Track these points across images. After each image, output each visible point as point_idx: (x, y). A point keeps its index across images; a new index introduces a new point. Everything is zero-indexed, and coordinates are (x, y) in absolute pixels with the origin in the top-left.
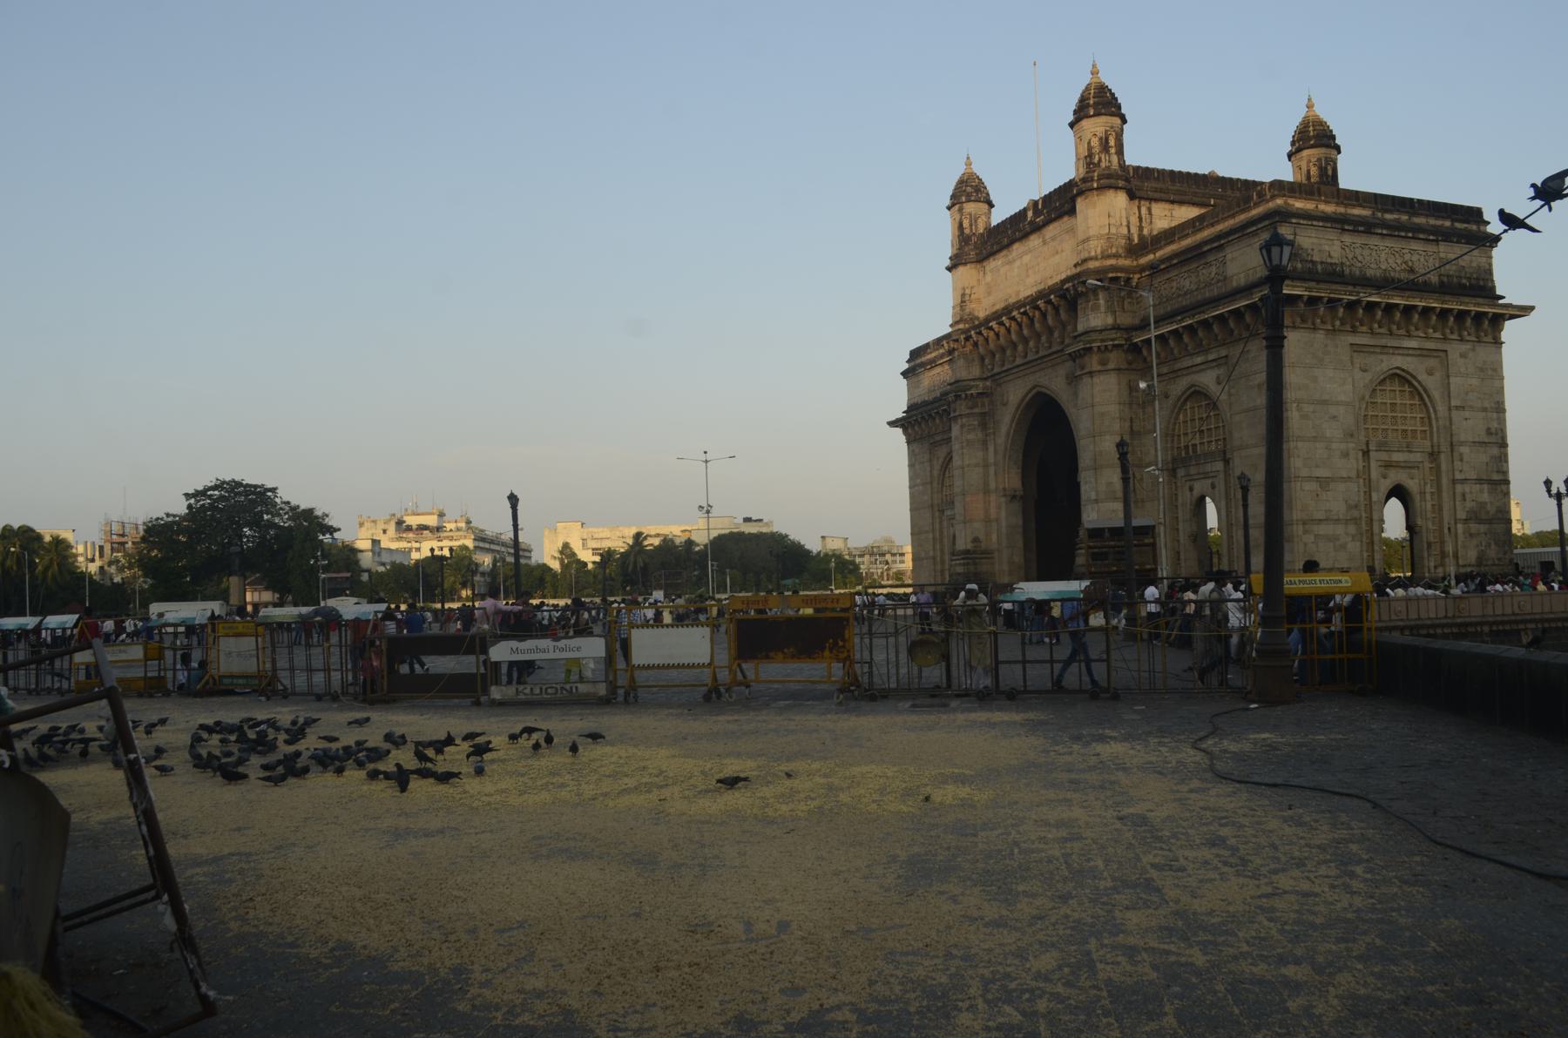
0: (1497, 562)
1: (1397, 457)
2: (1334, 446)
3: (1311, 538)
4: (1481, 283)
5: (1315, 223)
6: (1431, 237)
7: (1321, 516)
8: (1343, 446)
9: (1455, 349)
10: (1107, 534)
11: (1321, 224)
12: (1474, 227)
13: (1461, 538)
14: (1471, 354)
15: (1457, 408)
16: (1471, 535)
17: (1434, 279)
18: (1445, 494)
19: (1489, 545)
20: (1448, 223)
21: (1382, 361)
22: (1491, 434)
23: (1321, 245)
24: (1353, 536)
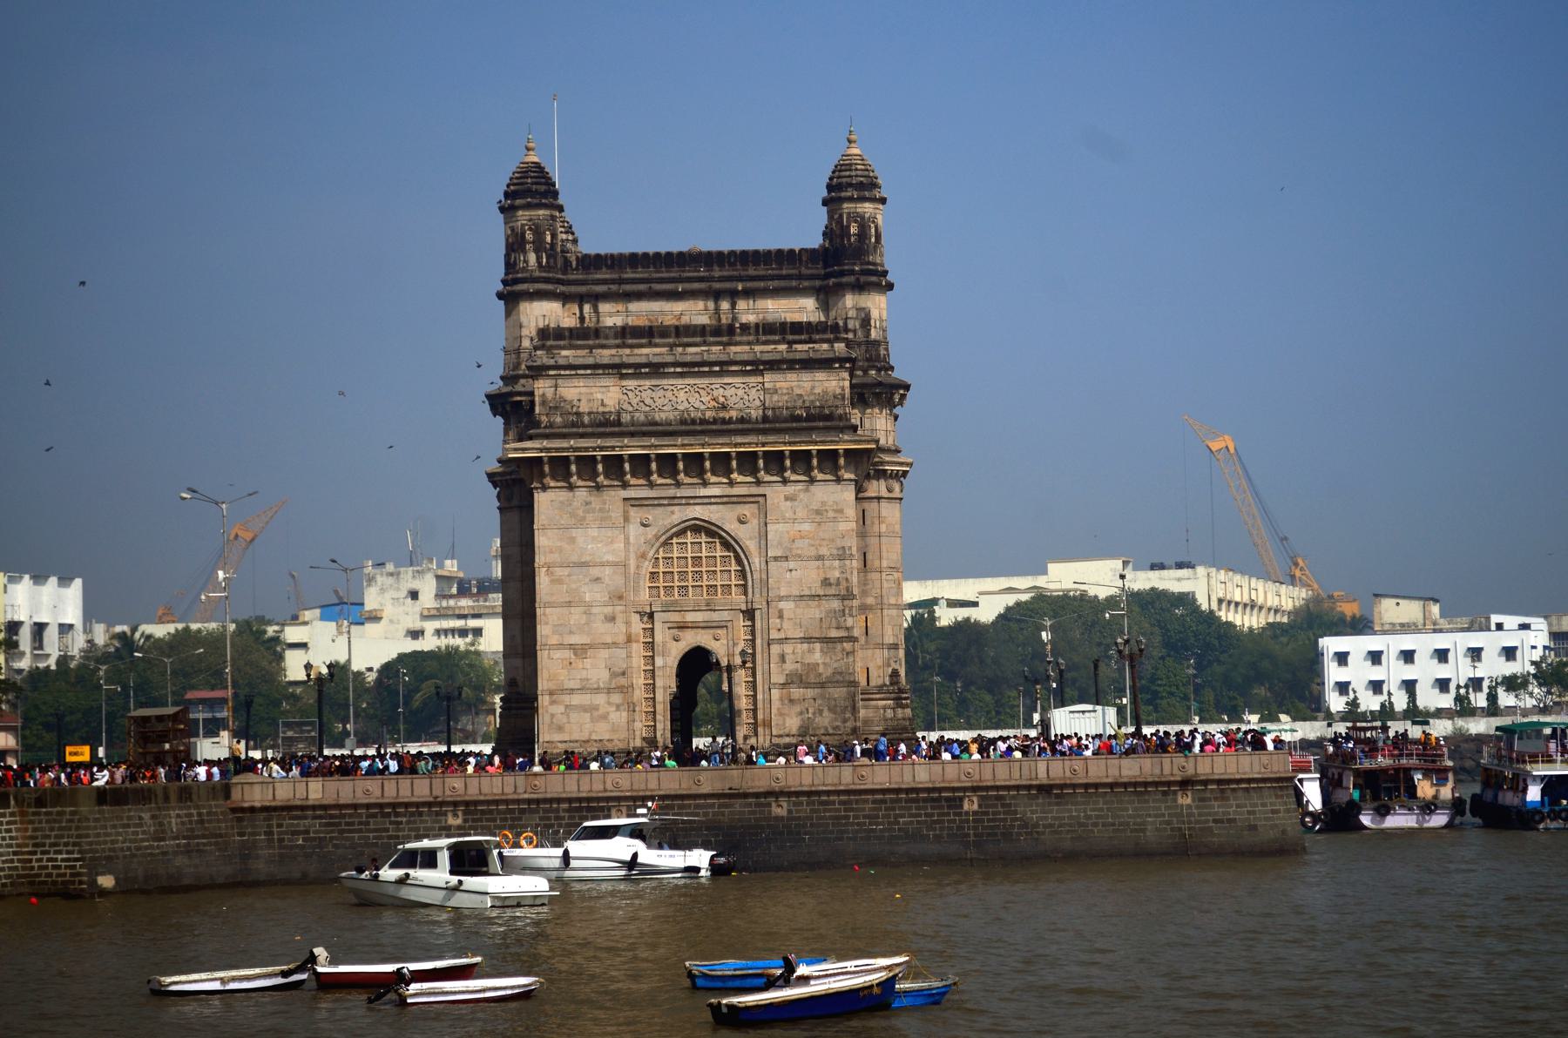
0: (831, 731)
1: (691, 617)
2: (595, 610)
3: (561, 709)
4: (827, 412)
5: (579, 372)
6: (748, 368)
7: (572, 685)
8: (608, 610)
9: (776, 494)
10: (153, 720)
11: (589, 372)
12: (825, 346)
13: (776, 704)
14: (802, 495)
15: (776, 559)
16: (791, 701)
17: (755, 414)
18: (759, 656)
19: (821, 712)
20: (783, 347)
21: (673, 513)
22: (830, 584)
23: (592, 394)
24: (618, 707)
